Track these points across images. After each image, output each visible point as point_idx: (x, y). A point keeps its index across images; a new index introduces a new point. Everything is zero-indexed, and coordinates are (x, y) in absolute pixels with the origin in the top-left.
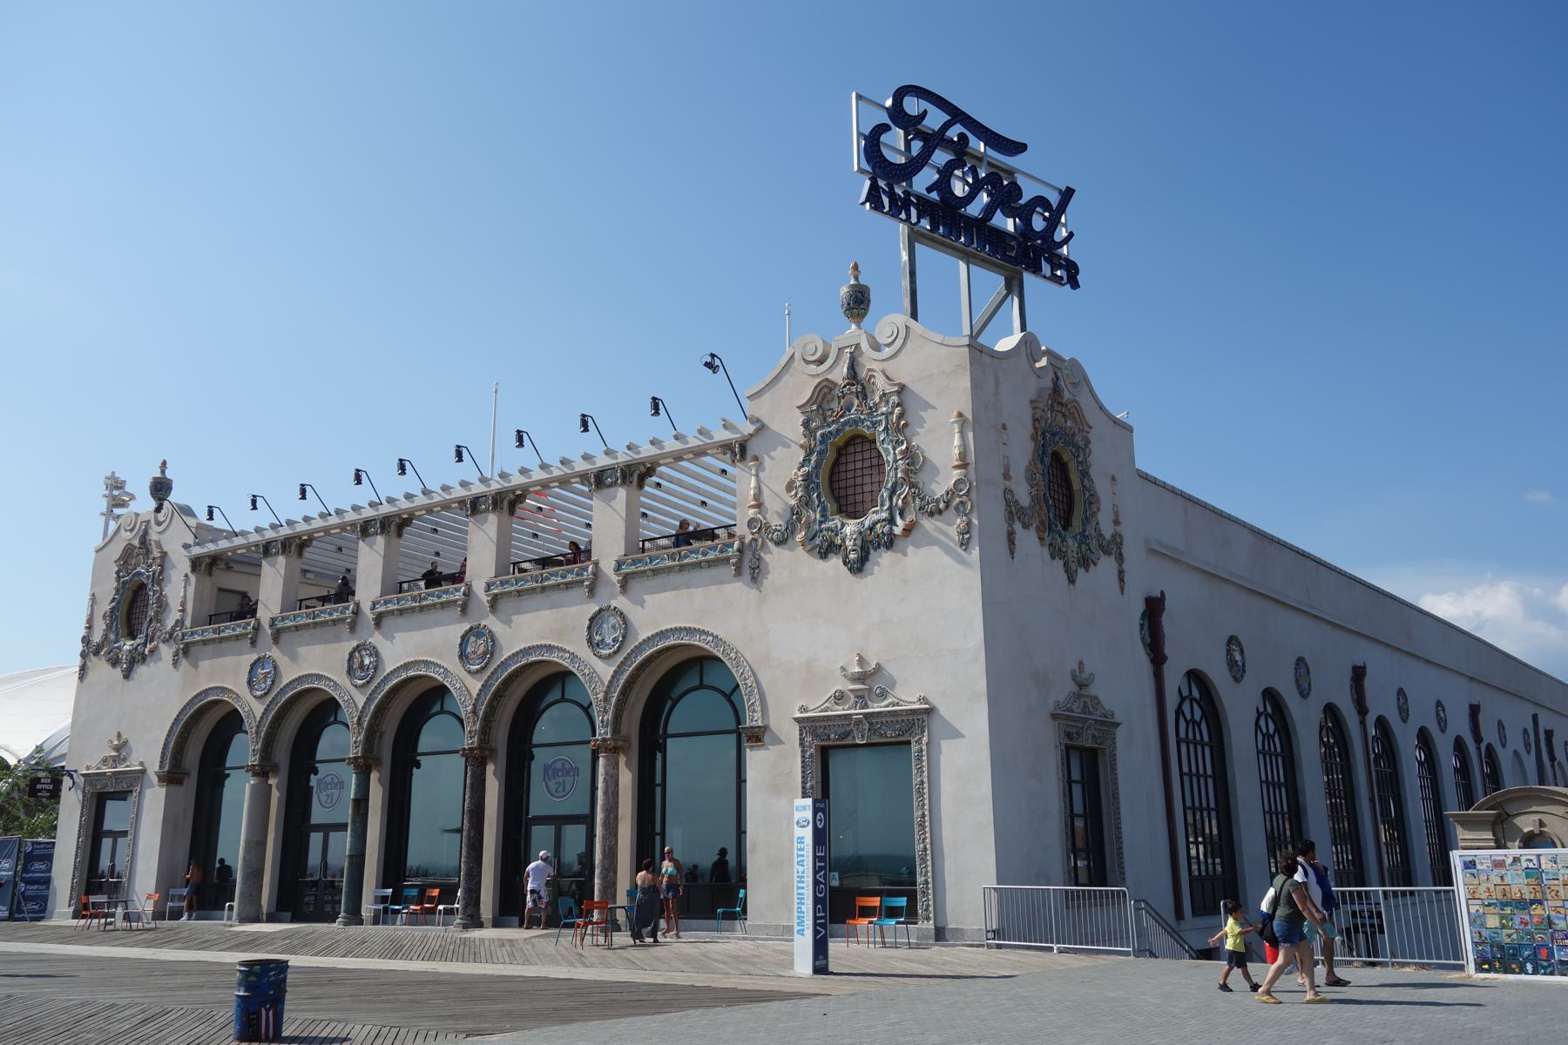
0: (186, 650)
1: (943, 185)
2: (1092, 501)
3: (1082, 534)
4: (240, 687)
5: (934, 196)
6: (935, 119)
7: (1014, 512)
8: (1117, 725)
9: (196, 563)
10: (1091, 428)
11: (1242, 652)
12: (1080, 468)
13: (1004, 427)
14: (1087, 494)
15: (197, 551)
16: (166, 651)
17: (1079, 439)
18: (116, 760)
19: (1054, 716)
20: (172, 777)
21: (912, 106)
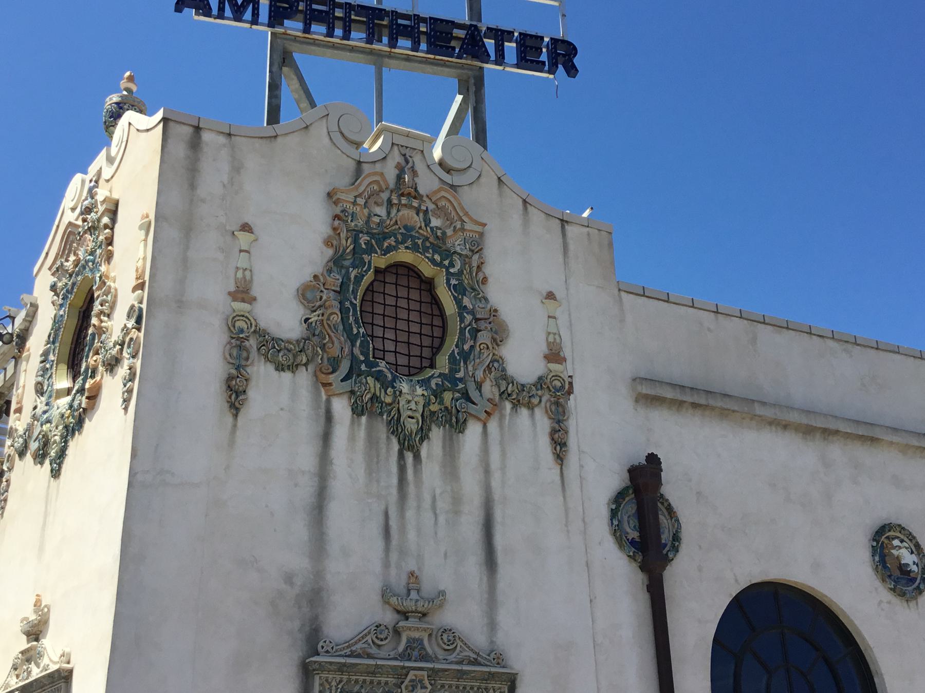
3: (451, 379)
10: (484, 225)
12: (453, 282)
13: (246, 228)
14: (469, 318)
17: (456, 243)
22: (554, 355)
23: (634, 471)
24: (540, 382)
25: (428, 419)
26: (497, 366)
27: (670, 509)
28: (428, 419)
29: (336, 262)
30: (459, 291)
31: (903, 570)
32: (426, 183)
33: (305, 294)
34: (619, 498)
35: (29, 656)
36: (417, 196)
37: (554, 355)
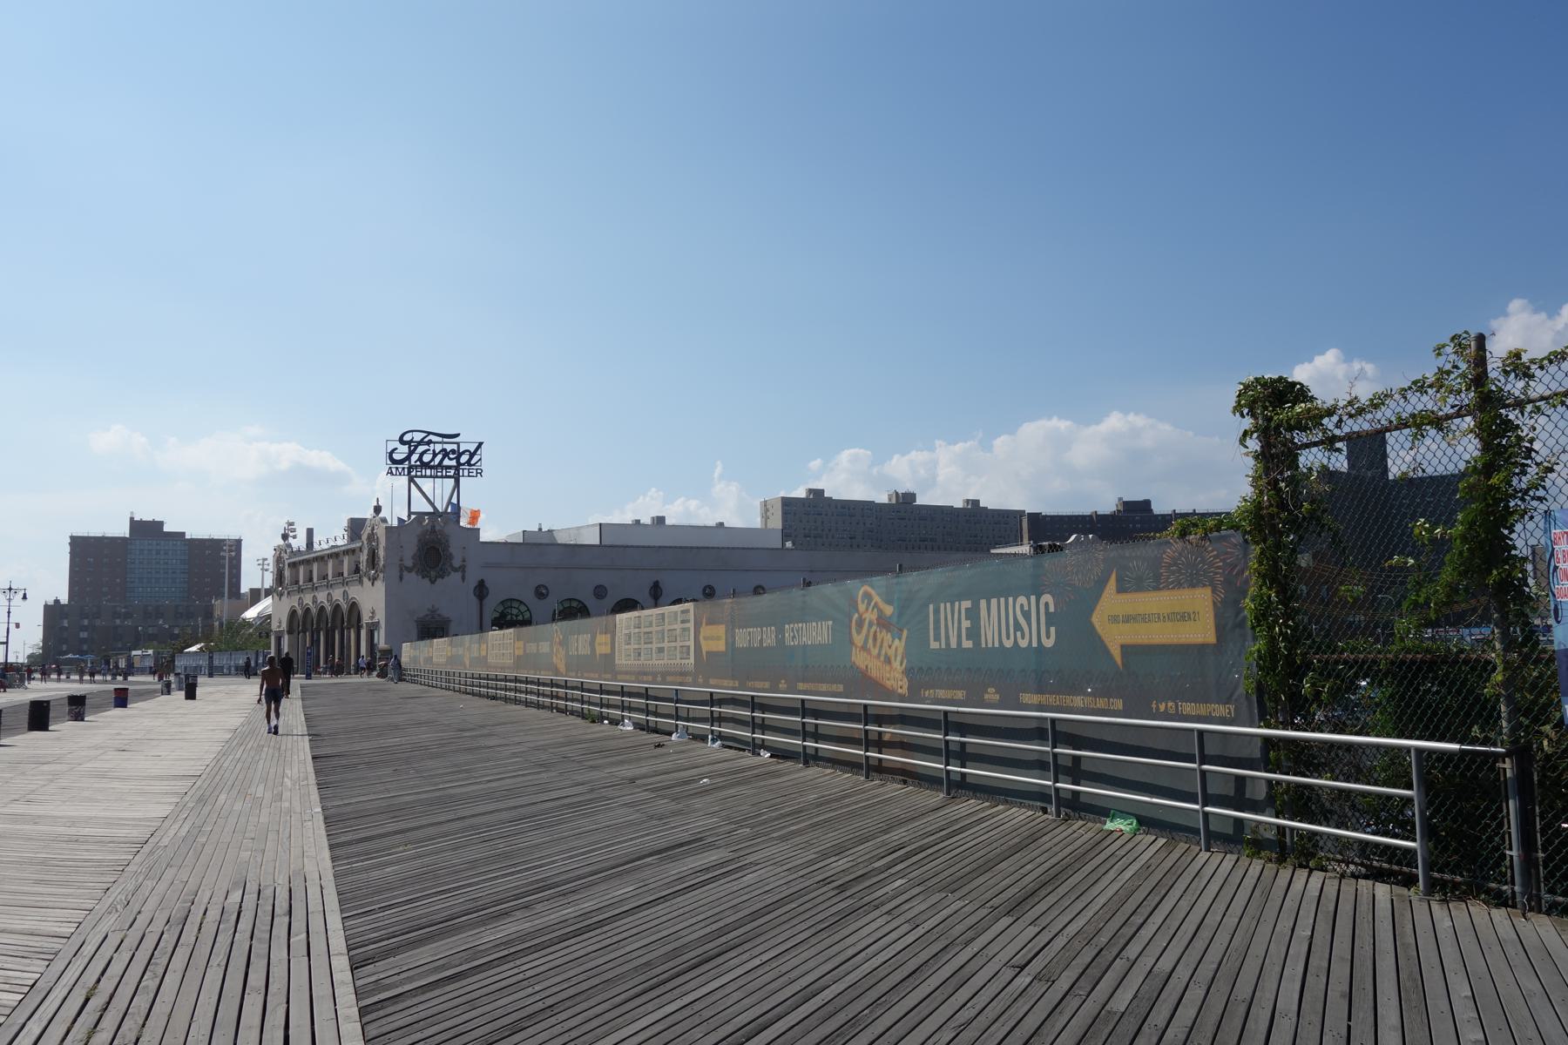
0: (288, 593)
1: (420, 459)
2: (450, 557)
3: (441, 569)
4: (297, 605)
5: (418, 463)
6: (418, 437)
7: (403, 569)
8: (450, 621)
9: (289, 565)
11: (547, 589)
13: (402, 547)
15: (289, 561)
16: (286, 592)
18: (279, 627)
19: (416, 621)
20: (290, 632)
21: (407, 438)
22: (464, 561)
23: (479, 582)
24: (460, 568)
25: (436, 577)
26: (451, 565)
27: (487, 589)
28: (436, 577)
29: (419, 549)
30: (443, 551)
31: (542, 594)
32: (437, 528)
33: (413, 558)
34: (476, 587)
35: (372, 618)
36: (435, 531)
37: (464, 561)
